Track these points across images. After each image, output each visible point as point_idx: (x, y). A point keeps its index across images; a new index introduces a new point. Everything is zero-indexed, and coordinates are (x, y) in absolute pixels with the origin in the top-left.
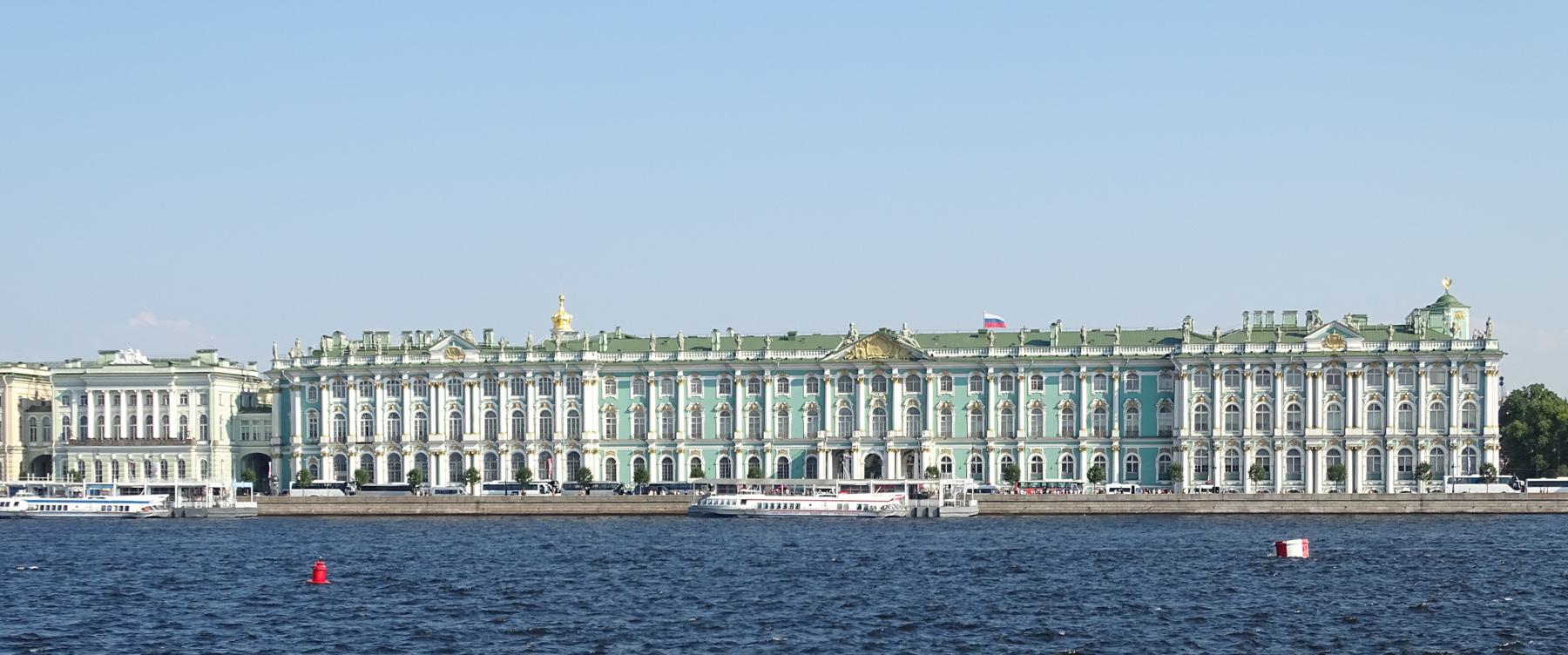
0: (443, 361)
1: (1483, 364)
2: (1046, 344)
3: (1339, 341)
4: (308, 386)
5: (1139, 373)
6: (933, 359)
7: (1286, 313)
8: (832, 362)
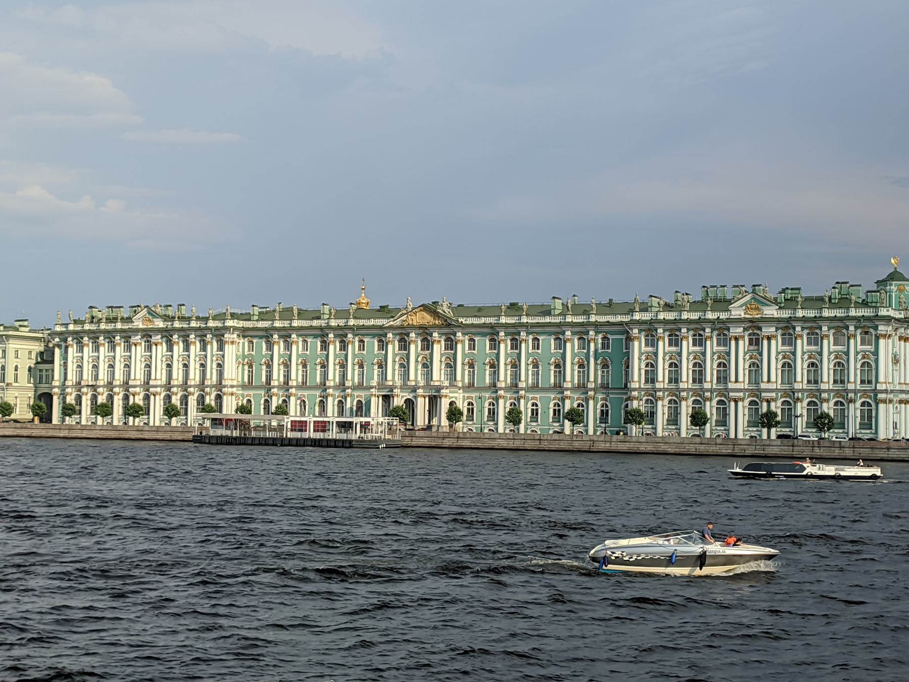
0: (141, 326)
1: (876, 328)
2: (548, 312)
3: (757, 309)
4: (63, 345)
5: (609, 336)
6: (461, 326)
7: (735, 286)
8: (391, 328)
